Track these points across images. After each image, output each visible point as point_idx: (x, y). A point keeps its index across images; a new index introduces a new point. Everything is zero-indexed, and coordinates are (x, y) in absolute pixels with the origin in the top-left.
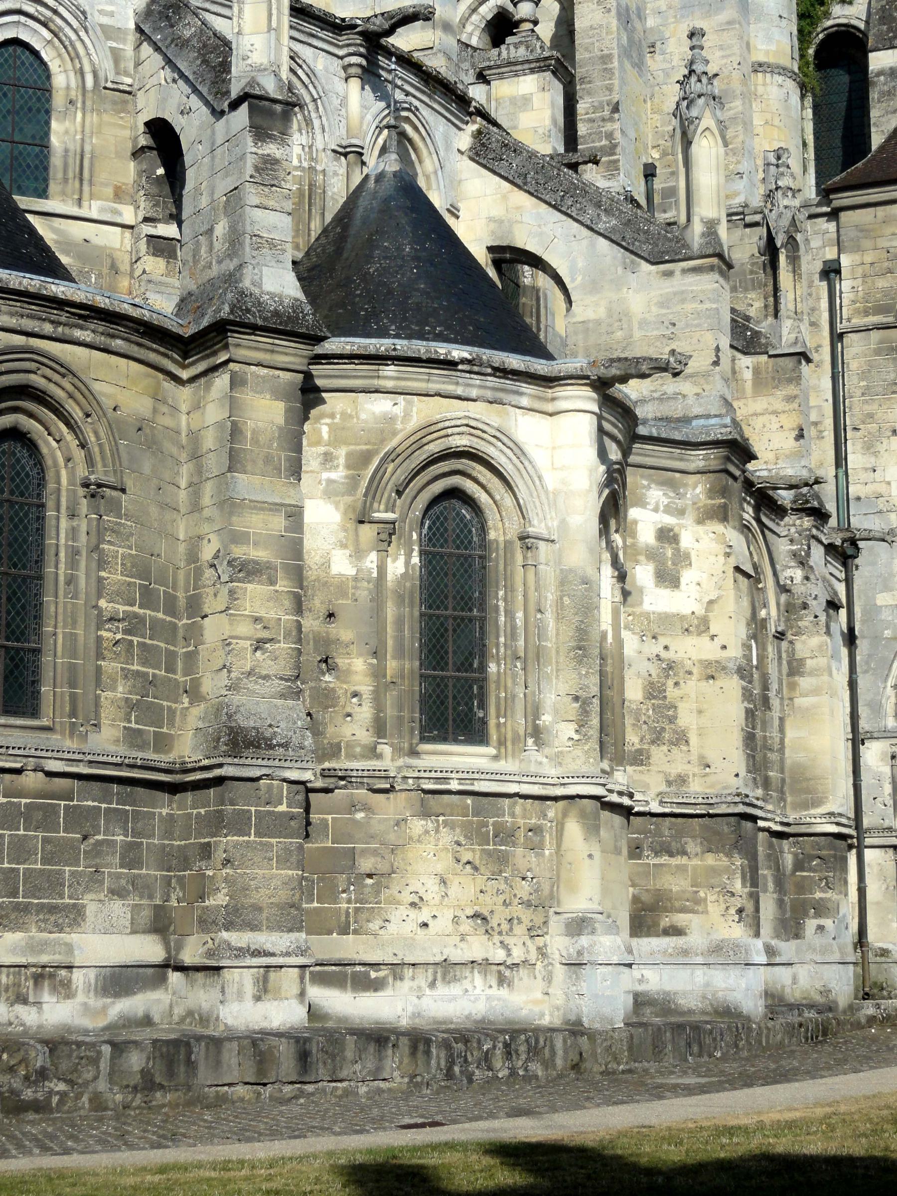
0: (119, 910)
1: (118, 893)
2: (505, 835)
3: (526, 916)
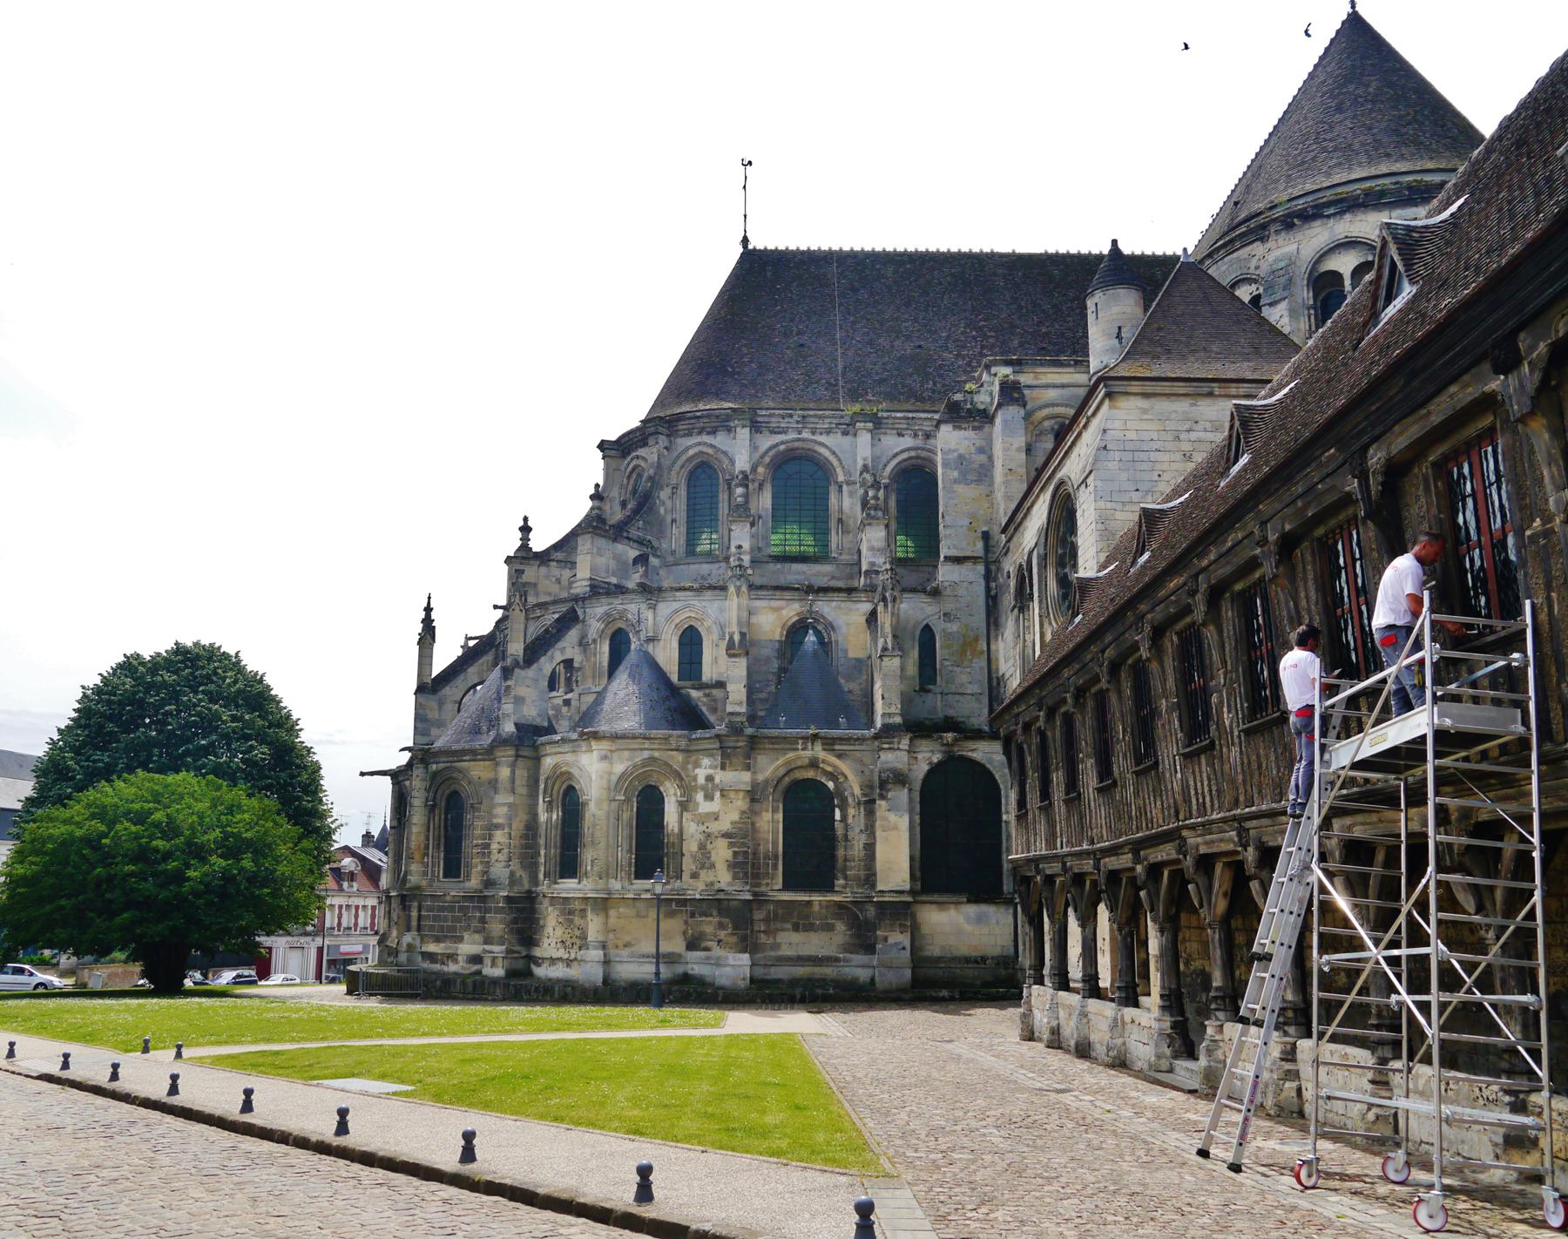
0: (477, 936)
2: (571, 912)
3: (578, 942)
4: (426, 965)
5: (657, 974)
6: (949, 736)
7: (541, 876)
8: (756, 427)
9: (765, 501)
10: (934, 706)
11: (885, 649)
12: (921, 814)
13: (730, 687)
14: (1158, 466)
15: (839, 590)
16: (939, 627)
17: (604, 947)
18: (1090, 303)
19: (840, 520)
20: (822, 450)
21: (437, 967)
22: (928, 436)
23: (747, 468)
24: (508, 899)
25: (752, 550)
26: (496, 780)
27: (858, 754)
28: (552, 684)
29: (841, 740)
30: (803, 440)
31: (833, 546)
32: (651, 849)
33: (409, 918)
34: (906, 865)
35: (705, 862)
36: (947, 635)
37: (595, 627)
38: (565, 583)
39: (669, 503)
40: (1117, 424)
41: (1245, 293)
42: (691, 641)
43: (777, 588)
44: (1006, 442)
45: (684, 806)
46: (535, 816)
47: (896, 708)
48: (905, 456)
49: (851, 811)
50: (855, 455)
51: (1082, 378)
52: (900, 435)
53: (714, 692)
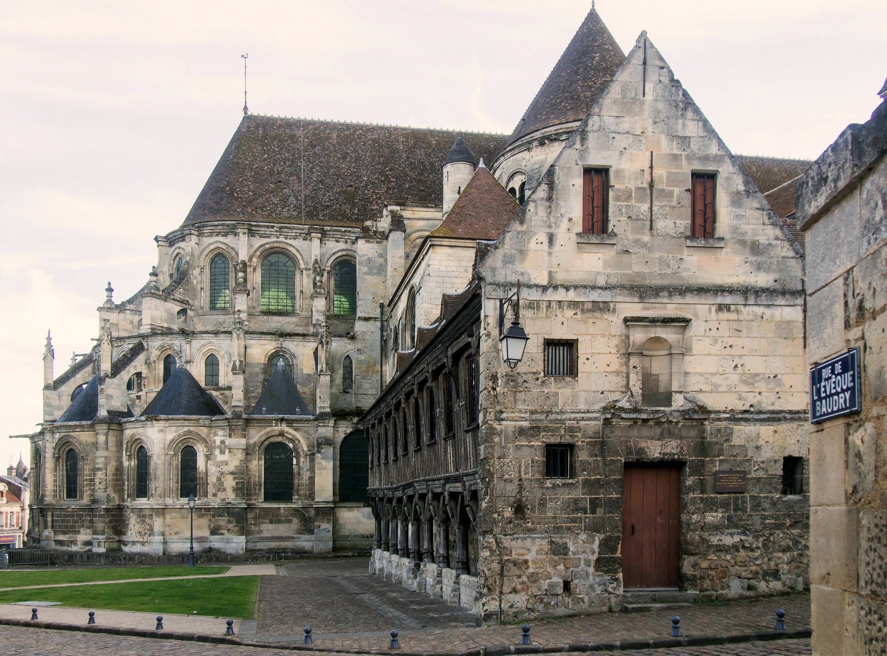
0: (88, 531)
1: (88, 528)
2: (144, 516)
3: (148, 532)
4: (58, 547)
5: (192, 548)
6: (356, 420)
7: (126, 497)
8: (251, 233)
9: (256, 278)
10: (351, 401)
11: (322, 371)
12: (340, 460)
13: (234, 391)
14: (455, 286)
15: (298, 335)
16: (354, 357)
17: (163, 535)
18: (445, 170)
19: (302, 292)
20: (291, 249)
21: (65, 548)
22: (354, 243)
23: (246, 259)
24: (107, 510)
25: (248, 307)
26: (97, 443)
27: (306, 429)
28: (129, 386)
29: (297, 421)
30: (280, 242)
31: (297, 307)
32: (189, 482)
33: (46, 522)
34: (331, 488)
35: (220, 487)
36: (359, 362)
37: (154, 353)
38: (136, 324)
39: (199, 278)
40: (436, 262)
41: (516, 183)
42: (212, 363)
43: (262, 333)
44: (396, 251)
45: (208, 457)
46: (121, 463)
47: (327, 404)
48: (340, 254)
49: (302, 460)
50: (311, 252)
51: (439, 215)
52: (337, 241)
53: (226, 392)
